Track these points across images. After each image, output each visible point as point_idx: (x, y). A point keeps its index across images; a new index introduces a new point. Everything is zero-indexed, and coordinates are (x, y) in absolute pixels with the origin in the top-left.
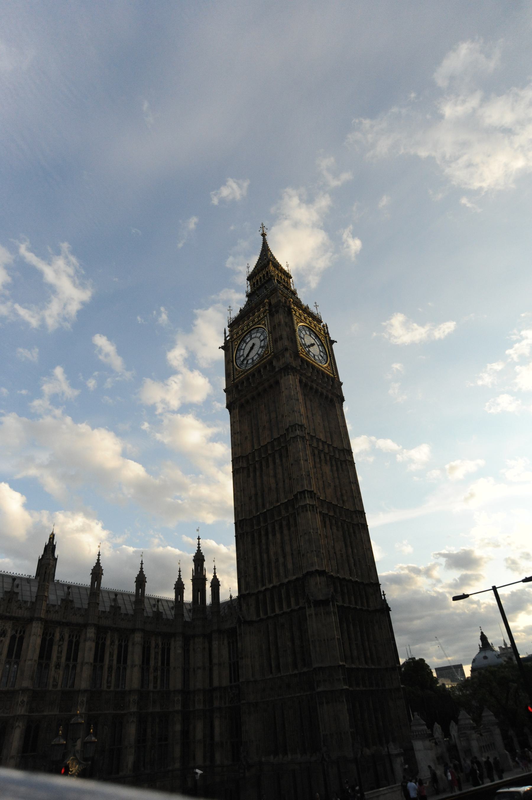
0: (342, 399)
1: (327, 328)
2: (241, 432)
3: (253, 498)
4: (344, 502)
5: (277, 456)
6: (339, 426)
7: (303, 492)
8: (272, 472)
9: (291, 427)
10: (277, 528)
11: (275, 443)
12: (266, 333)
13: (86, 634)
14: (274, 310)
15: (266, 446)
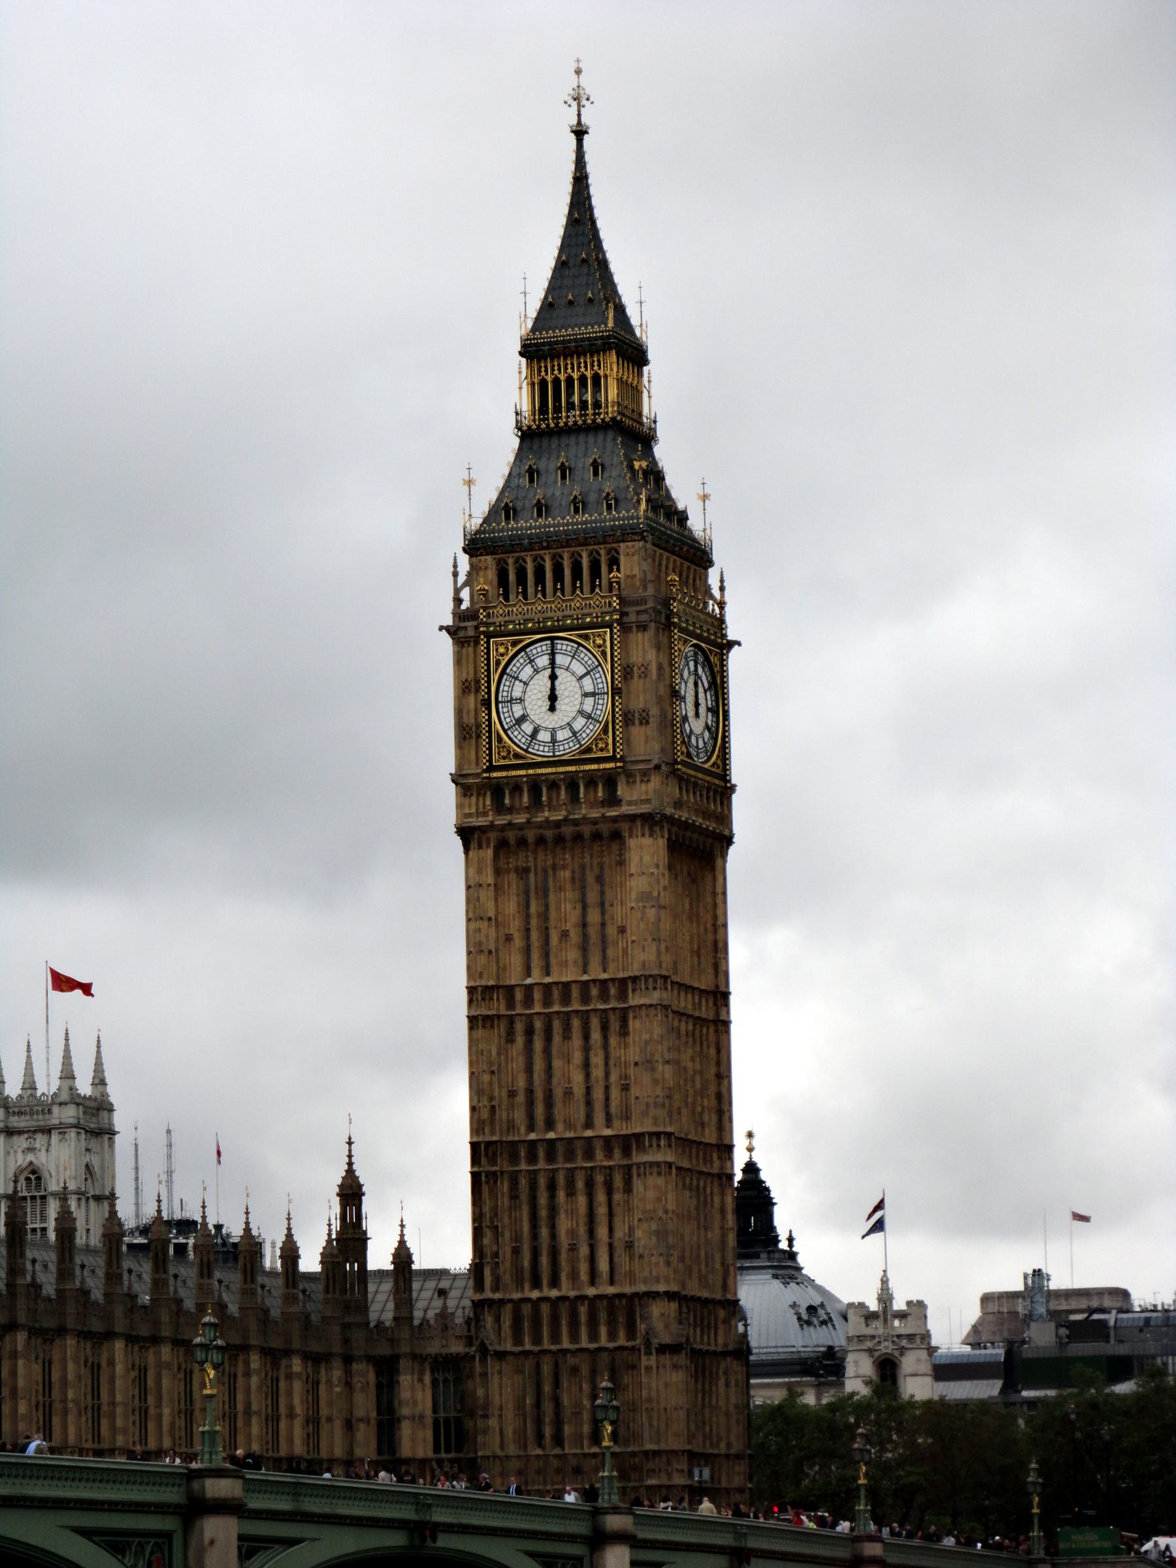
0: (728, 840)
1: (722, 589)
2: (496, 919)
3: (521, 1098)
4: (703, 1125)
5: (595, 1023)
6: (714, 925)
7: (657, 1135)
8: (577, 1057)
9: (647, 977)
10: (580, 1184)
11: (594, 992)
12: (603, 680)
13: (247, 1363)
14: (632, 618)
15: (567, 986)
